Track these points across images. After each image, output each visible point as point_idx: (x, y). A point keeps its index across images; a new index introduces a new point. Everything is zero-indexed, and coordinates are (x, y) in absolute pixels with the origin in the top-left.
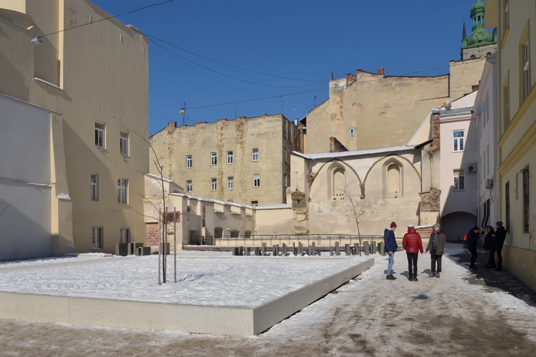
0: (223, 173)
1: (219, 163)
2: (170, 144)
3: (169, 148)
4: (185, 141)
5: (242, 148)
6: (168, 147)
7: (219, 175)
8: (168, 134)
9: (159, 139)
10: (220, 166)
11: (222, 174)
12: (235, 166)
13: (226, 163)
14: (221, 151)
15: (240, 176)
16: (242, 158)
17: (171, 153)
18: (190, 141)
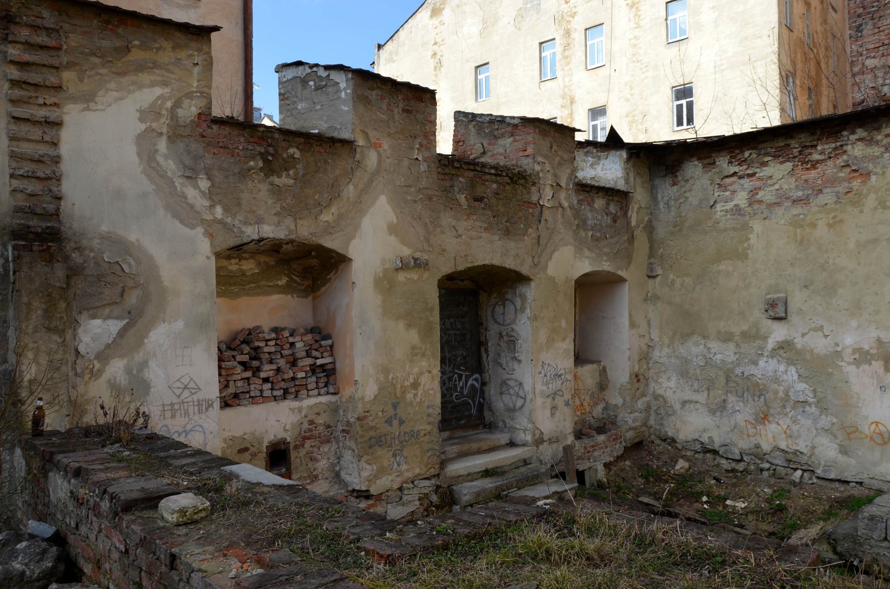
0: (576, 99)
1: (563, 69)
2: (435, 44)
3: (435, 54)
4: (472, 27)
5: (632, 7)
6: (430, 53)
7: (562, 107)
8: (431, 17)
9: (412, 35)
10: (567, 80)
11: (572, 102)
12: (613, 70)
13: (583, 67)
14: (568, 33)
15: (627, 100)
16: (634, 41)
17: (439, 65)
18: (484, 22)
